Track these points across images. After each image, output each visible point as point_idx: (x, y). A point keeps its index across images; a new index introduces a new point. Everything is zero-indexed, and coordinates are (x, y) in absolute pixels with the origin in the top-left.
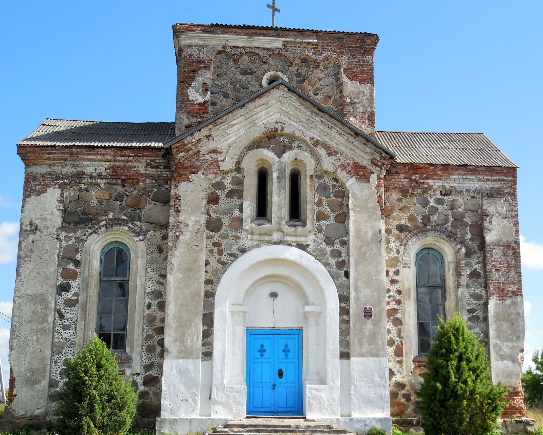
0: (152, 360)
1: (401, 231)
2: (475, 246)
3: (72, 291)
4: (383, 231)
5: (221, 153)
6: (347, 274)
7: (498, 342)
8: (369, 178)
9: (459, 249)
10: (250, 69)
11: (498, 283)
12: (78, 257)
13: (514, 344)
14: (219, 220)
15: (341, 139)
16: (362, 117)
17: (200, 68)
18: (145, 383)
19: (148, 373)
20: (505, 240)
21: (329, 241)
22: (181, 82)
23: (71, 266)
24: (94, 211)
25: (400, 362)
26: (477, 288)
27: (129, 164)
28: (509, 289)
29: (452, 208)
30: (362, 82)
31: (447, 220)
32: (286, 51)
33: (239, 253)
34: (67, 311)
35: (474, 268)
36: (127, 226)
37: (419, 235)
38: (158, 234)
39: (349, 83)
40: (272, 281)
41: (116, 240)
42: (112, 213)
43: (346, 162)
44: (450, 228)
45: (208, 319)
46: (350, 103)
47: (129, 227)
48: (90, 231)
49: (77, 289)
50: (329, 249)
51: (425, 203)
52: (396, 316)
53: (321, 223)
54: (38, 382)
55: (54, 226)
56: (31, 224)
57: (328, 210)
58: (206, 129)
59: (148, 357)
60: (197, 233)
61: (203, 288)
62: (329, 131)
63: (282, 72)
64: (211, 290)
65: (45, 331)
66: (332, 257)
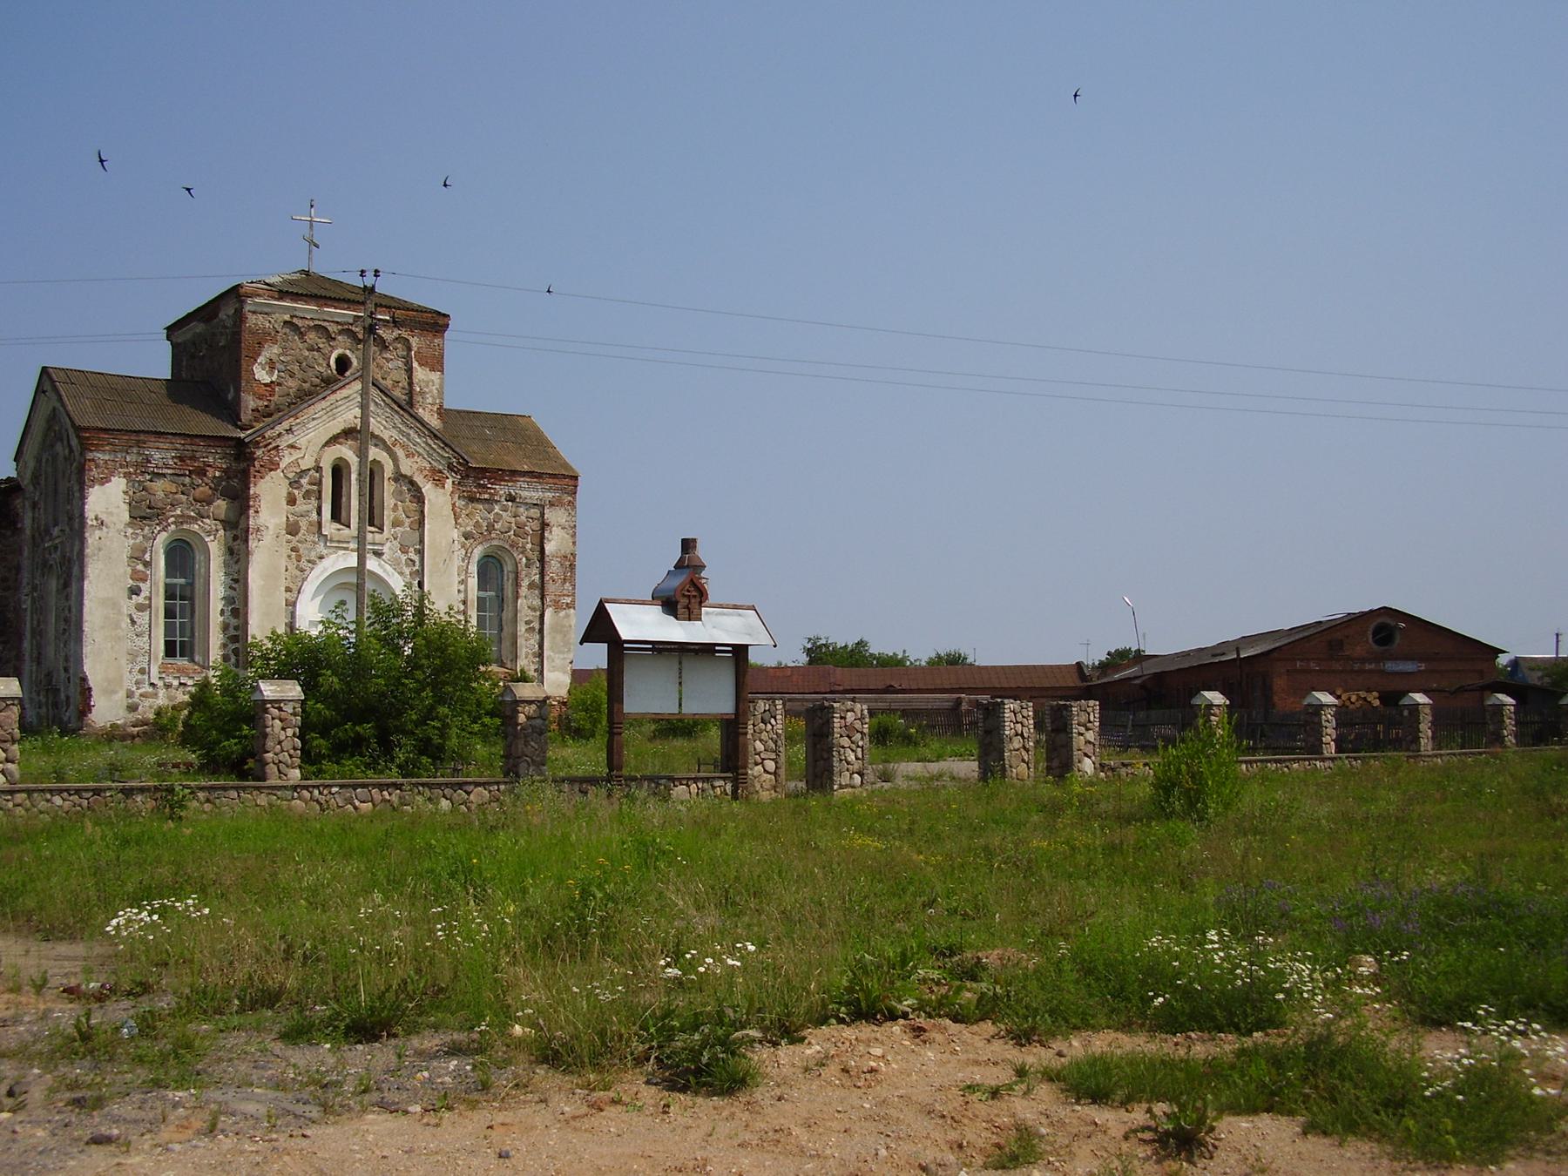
2: (535, 556)
23: (140, 567)
24: (160, 505)
30: (432, 370)
50: (404, 558)
54: (114, 692)
61: (282, 596)
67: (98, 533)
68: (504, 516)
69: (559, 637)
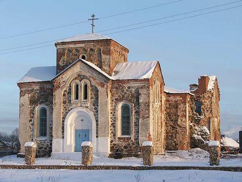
21: (94, 105)
25: (115, 138)
29: (131, 92)
31: (129, 96)
51: (123, 91)
69: (144, 127)
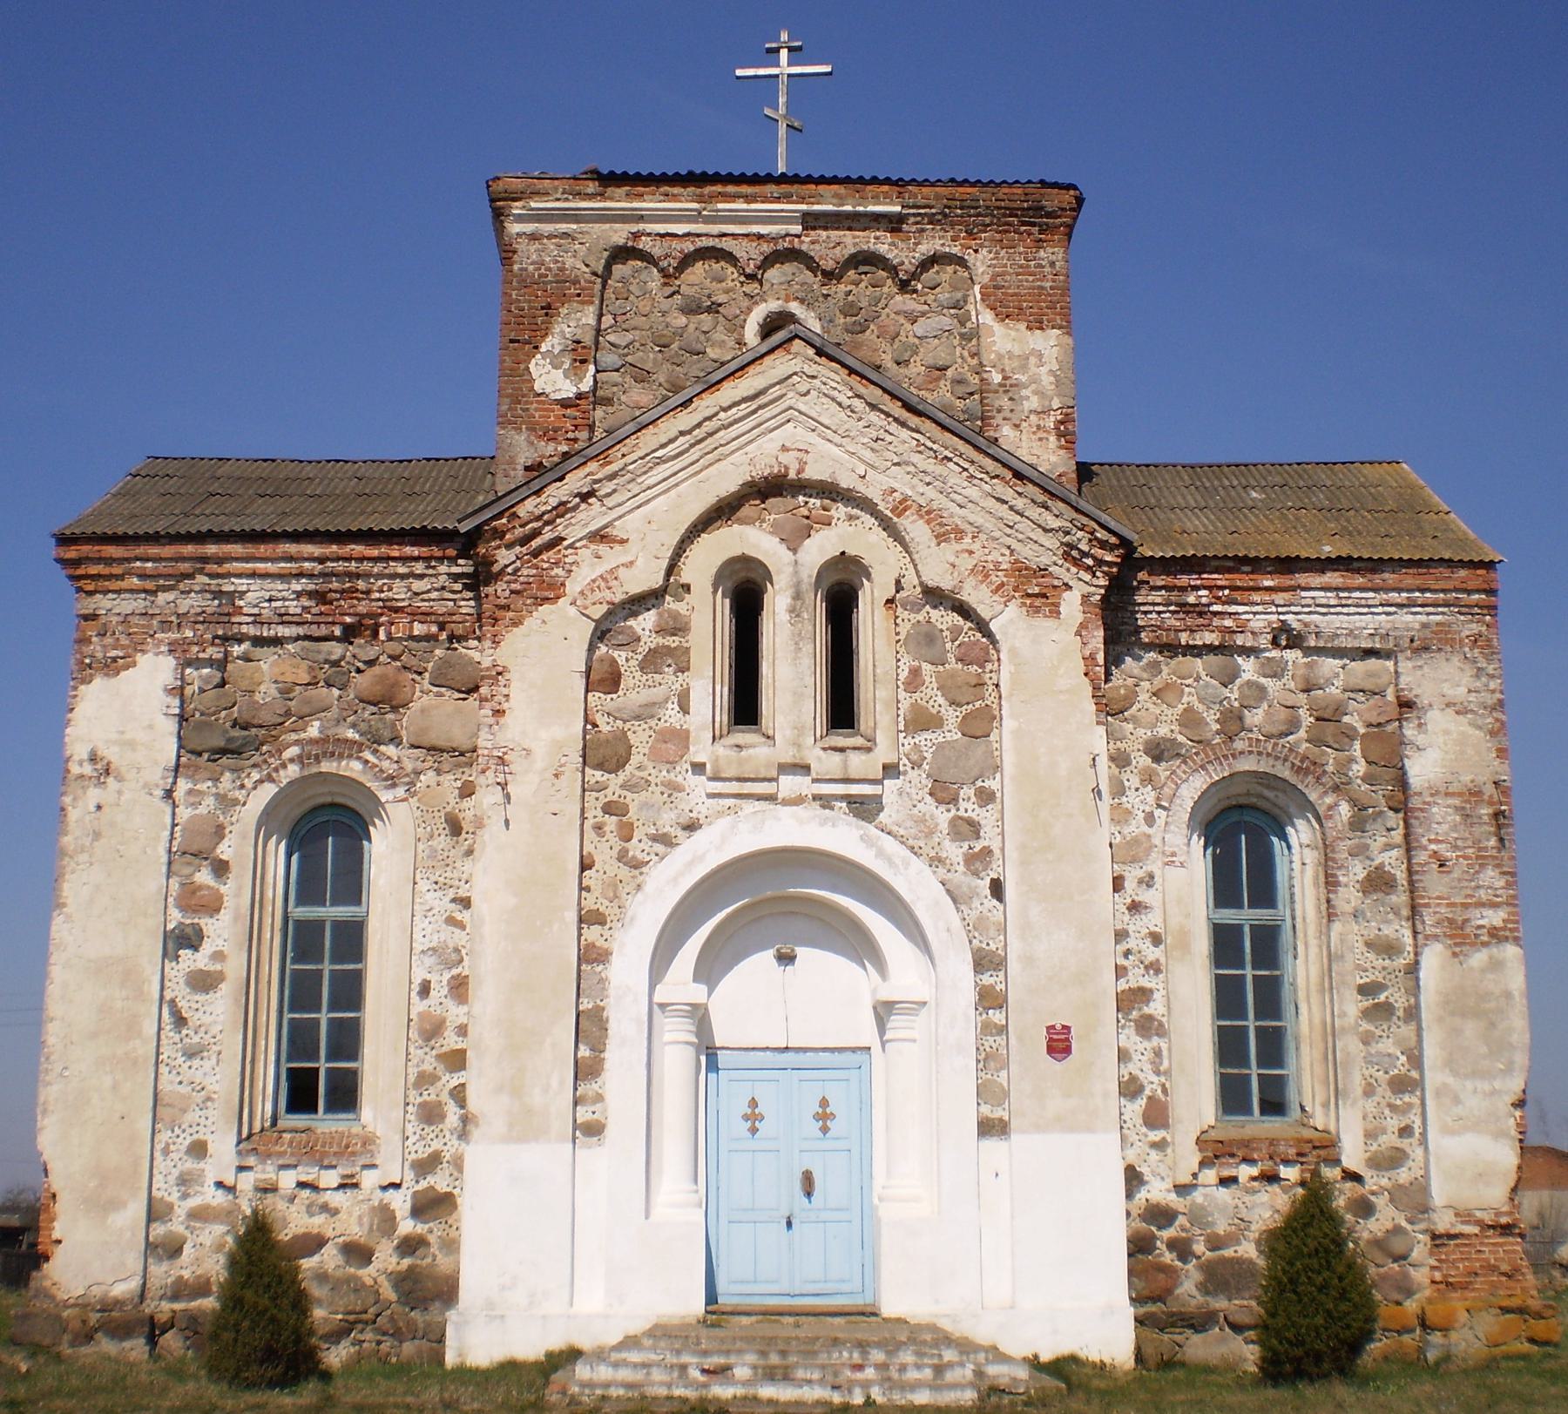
0: (436, 1145)
1: (1157, 759)
3: (207, 948)
4: (1103, 762)
5: (623, 542)
6: (997, 889)
7: (1450, 1080)
8: (1057, 605)
9: (1330, 808)
10: (709, 297)
11: (1448, 905)
12: (225, 851)
13: (1497, 1084)
14: (622, 736)
15: (973, 492)
16: (1039, 427)
17: (564, 298)
18: (418, 1211)
19: (423, 1185)
20: (1467, 778)
21: (943, 792)
22: (512, 341)
23: (204, 877)
24: (266, 717)
26: (1388, 922)
27: (361, 585)
28: (1481, 922)
30: (1037, 324)
31: (1293, 725)
32: (813, 243)
33: (680, 833)
34: (195, 1006)
35: (1377, 862)
36: (359, 758)
37: (1210, 768)
38: (451, 783)
39: (997, 327)
40: (785, 913)
41: (329, 799)
42: (317, 724)
43: (990, 558)
44: (1306, 745)
45: (590, 1027)
46: (1000, 385)
47: (367, 762)
48: (256, 776)
49: (220, 942)
50: (943, 816)
52: (1146, 1010)
53: (921, 738)
54: (115, 1205)
55: (156, 763)
56: (93, 758)
57: (941, 700)
58: (581, 472)
59: (422, 1138)
60: (556, 776)
62: (939, 469)
63: (802, 301)
64: (600, 943)
65: (135, 1063)
66: (952, 840)
67: (94, 795)
68: (1272, 688)
69: (1471, 1029)
